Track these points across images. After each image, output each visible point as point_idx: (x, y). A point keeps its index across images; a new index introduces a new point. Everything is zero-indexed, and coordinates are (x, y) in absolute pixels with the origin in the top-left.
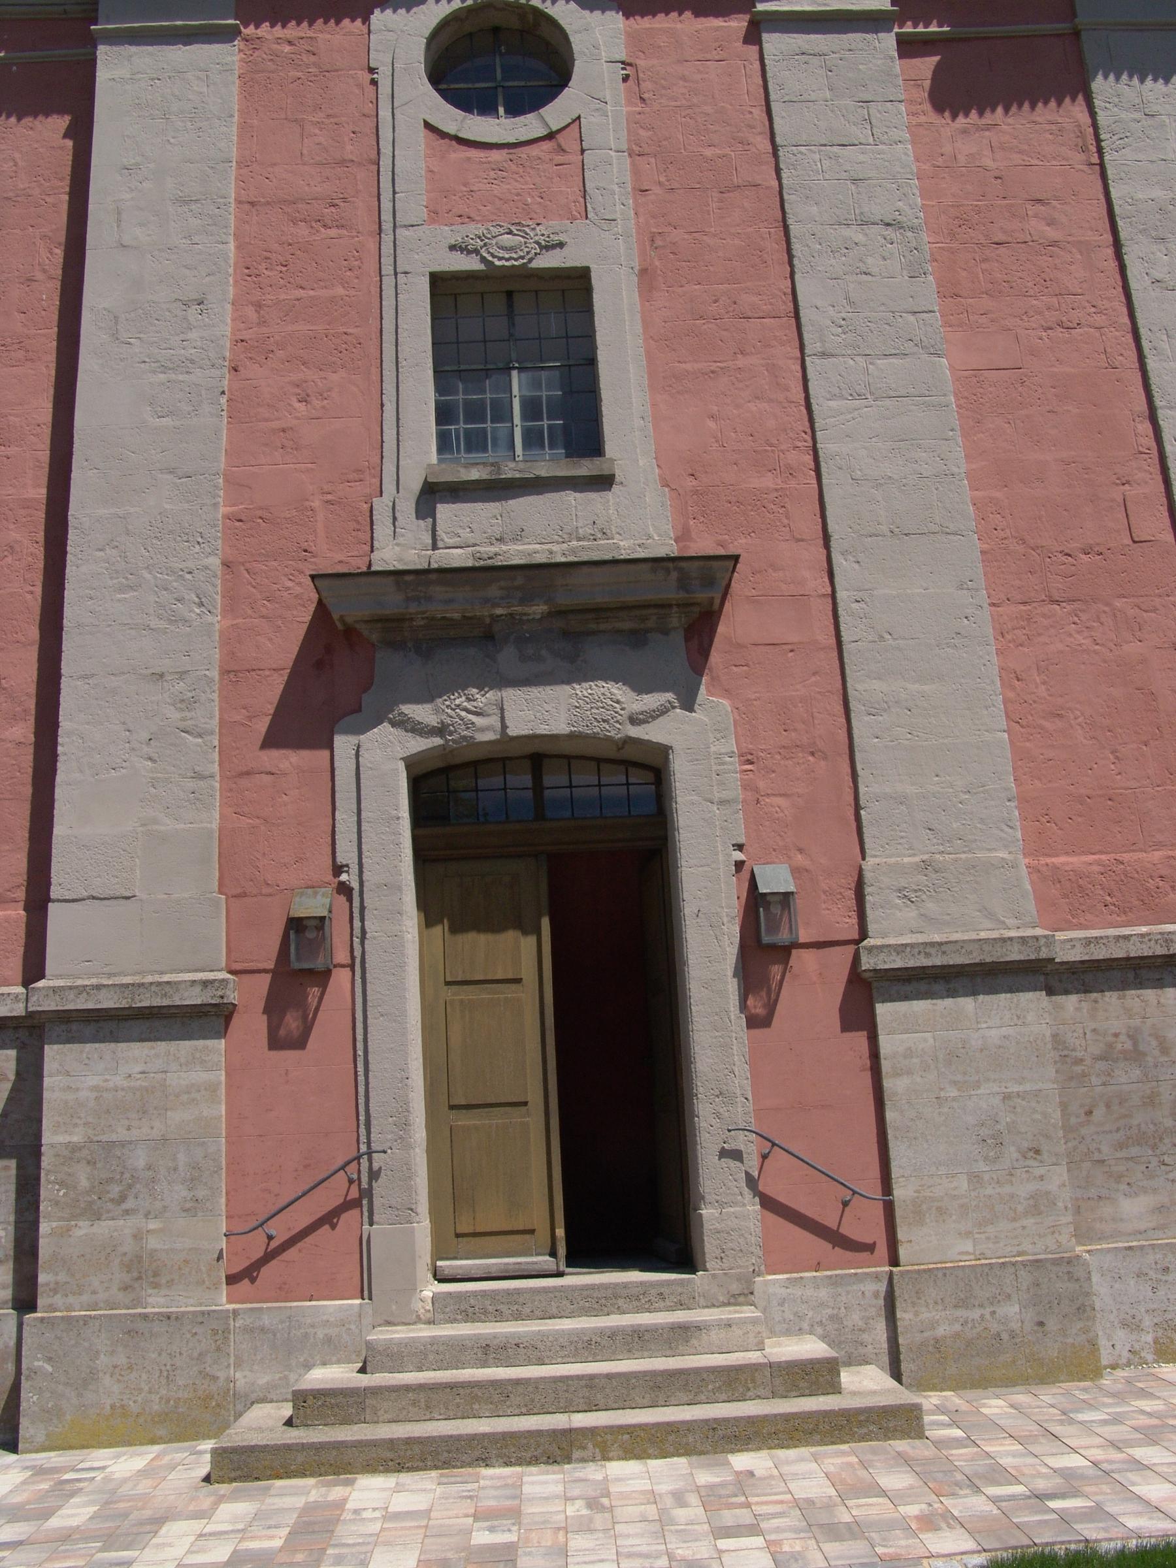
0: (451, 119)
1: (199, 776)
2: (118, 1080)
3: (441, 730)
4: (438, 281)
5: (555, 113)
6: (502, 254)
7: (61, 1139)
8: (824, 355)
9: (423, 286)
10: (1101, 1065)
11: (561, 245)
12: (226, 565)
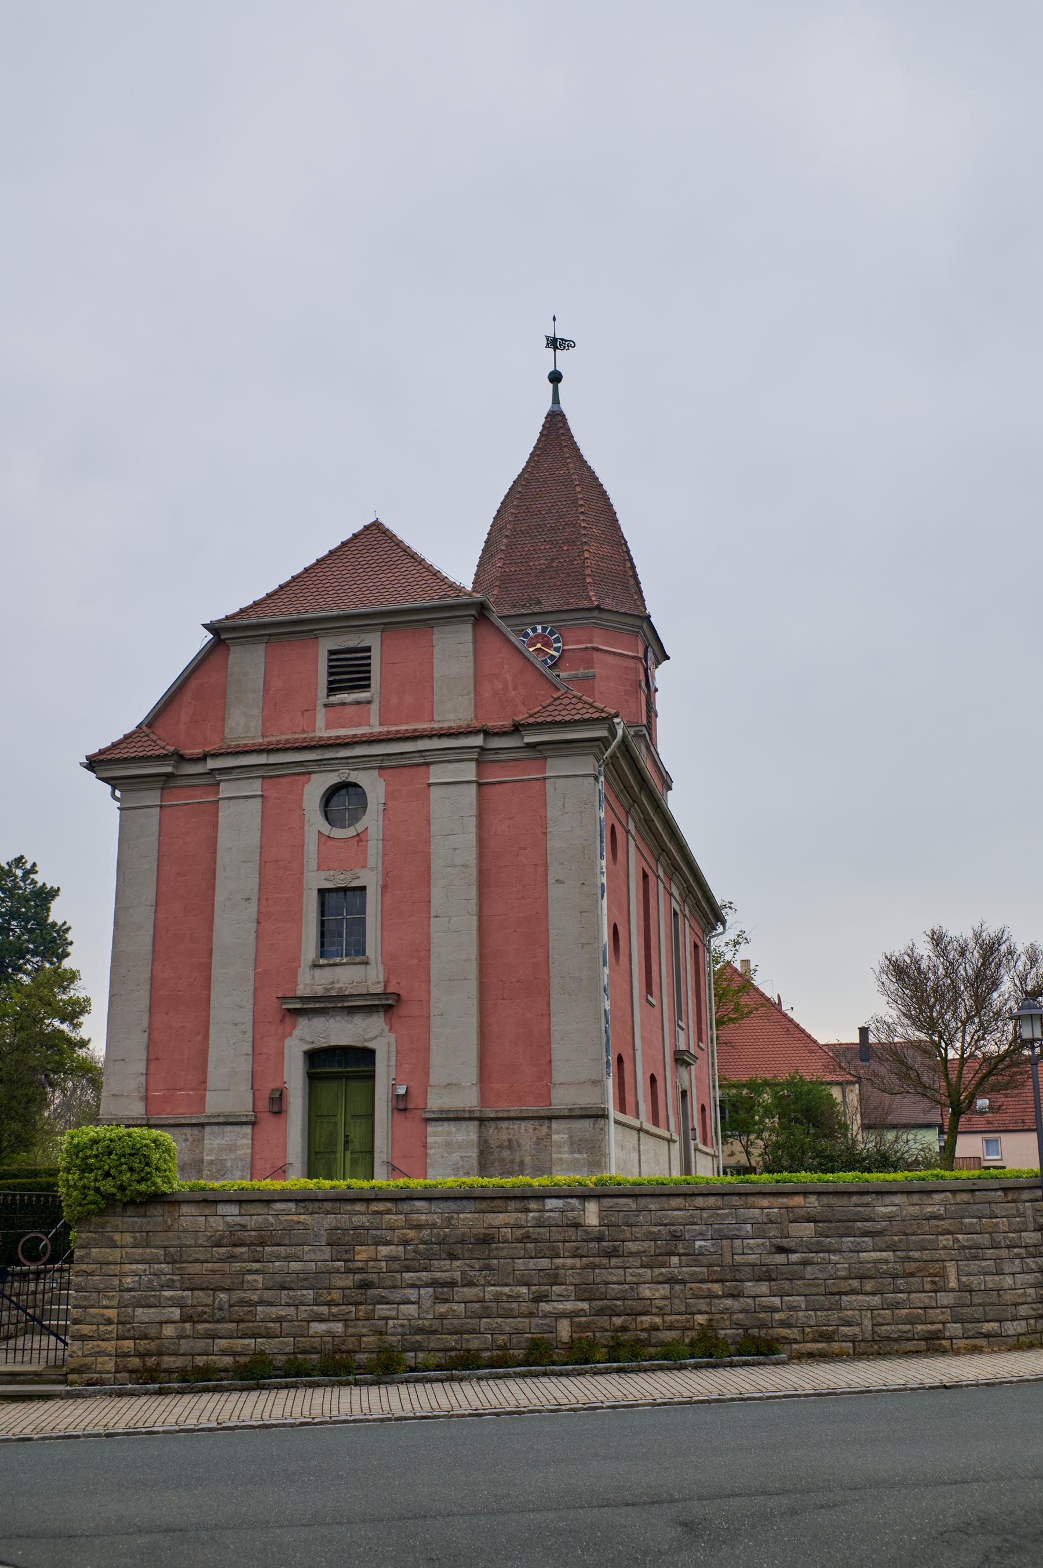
0: (326, 828)
1: (247, 1055)
2: (224, 1142)
3: (313, 1043)
4: (322, 892)
5: (360, 827)
6: (340, 882)
7: (209, 1158)
8: (437, 917)
9: (314, 894)
10: (498, 1149)
11: (359, 878)
12: (255, 989)
